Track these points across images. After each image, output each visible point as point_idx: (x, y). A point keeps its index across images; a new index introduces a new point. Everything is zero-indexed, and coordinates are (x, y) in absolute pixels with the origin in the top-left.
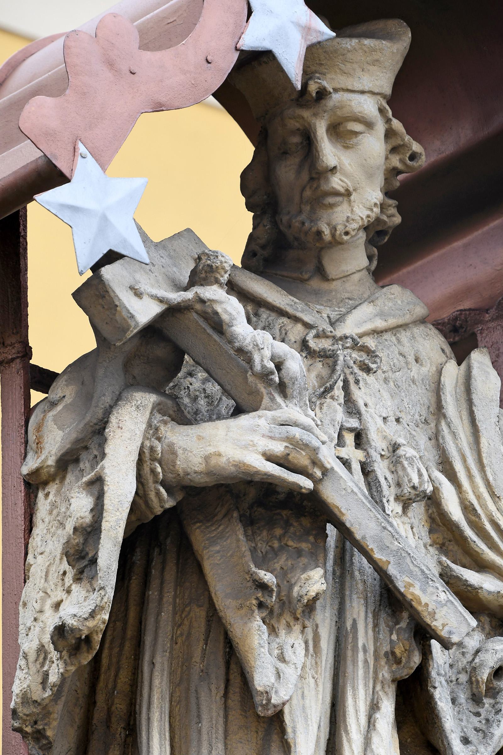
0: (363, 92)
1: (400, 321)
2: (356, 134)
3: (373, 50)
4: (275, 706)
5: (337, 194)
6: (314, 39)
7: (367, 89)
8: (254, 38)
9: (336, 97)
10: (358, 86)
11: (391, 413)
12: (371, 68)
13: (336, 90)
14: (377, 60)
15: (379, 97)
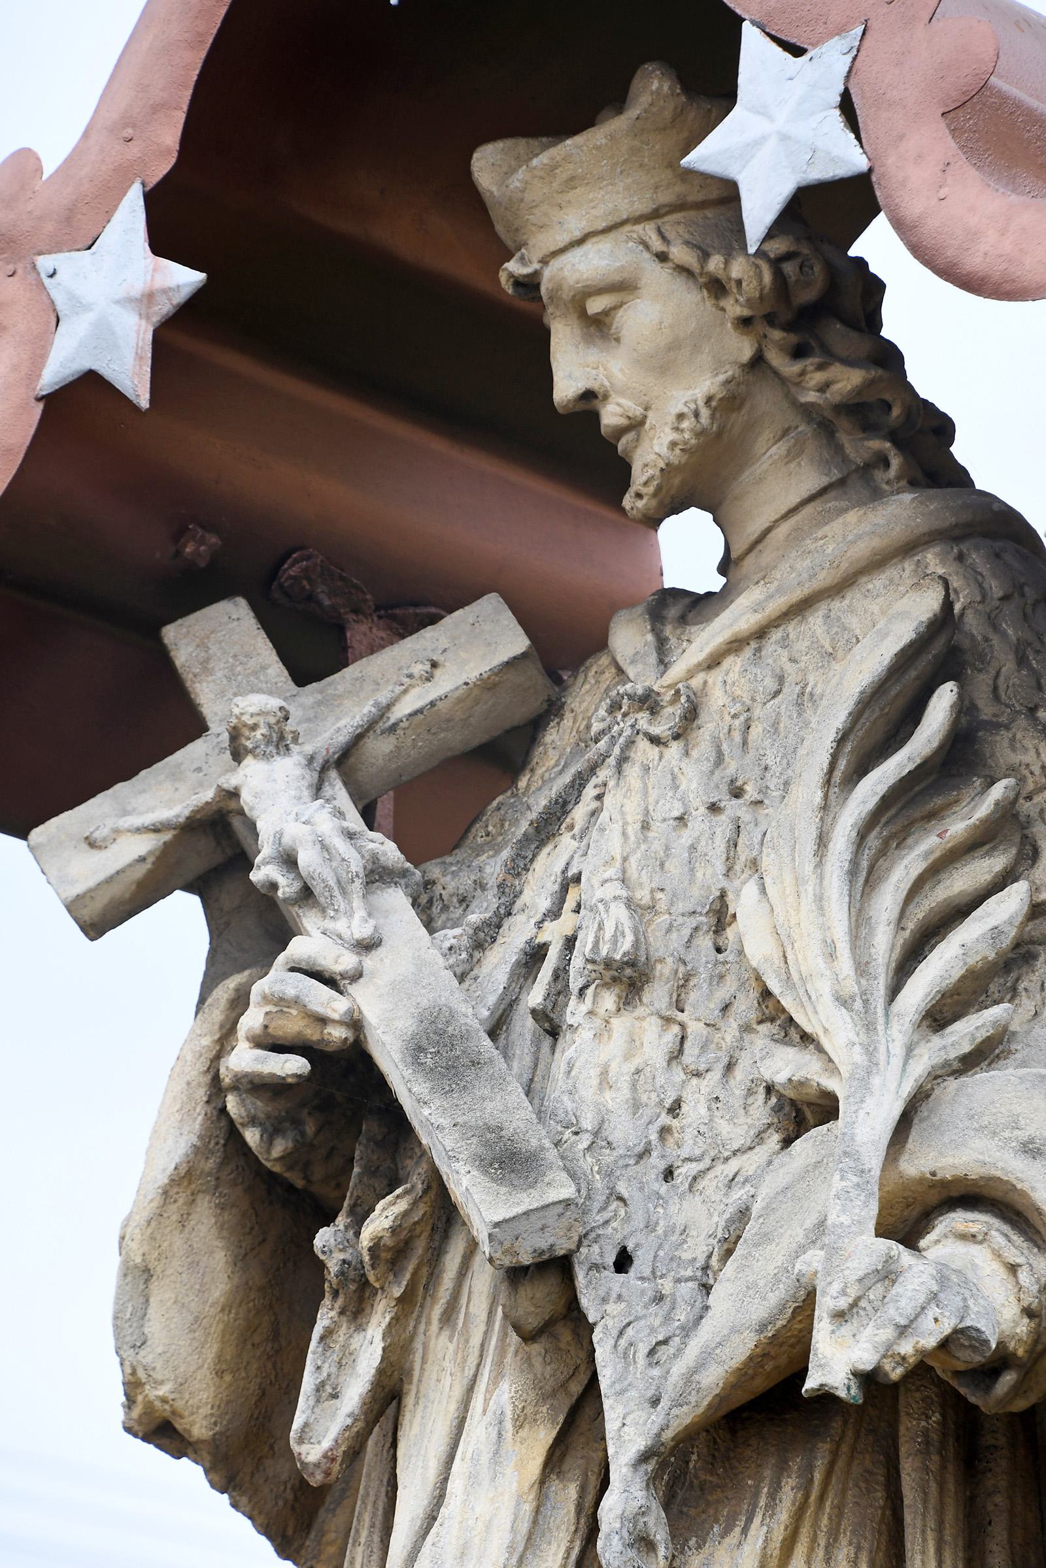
0: (580, 242)
1: (797, 595)
2: (607, 313)
3: (552, 168)
4: (317, 1465)
5: (621, 431)
6: (164, 308)
7: (578, 234)
8: (59, 366)
9: (547, 273)
10: (562, 239)
11: (696, 802)
12: (571, 195)
13: (544, 261)
14: (572, 178)
15: (628, 228)
